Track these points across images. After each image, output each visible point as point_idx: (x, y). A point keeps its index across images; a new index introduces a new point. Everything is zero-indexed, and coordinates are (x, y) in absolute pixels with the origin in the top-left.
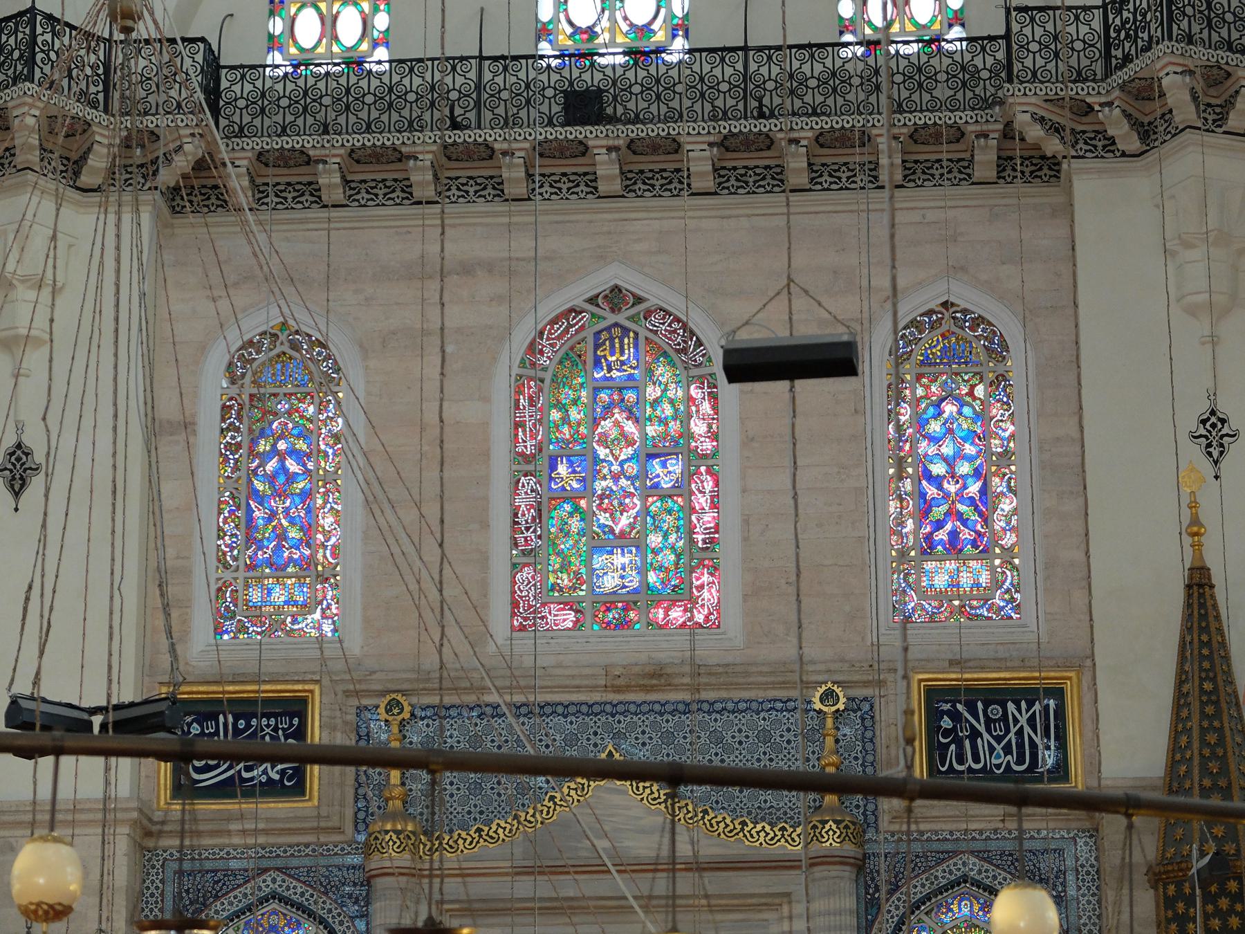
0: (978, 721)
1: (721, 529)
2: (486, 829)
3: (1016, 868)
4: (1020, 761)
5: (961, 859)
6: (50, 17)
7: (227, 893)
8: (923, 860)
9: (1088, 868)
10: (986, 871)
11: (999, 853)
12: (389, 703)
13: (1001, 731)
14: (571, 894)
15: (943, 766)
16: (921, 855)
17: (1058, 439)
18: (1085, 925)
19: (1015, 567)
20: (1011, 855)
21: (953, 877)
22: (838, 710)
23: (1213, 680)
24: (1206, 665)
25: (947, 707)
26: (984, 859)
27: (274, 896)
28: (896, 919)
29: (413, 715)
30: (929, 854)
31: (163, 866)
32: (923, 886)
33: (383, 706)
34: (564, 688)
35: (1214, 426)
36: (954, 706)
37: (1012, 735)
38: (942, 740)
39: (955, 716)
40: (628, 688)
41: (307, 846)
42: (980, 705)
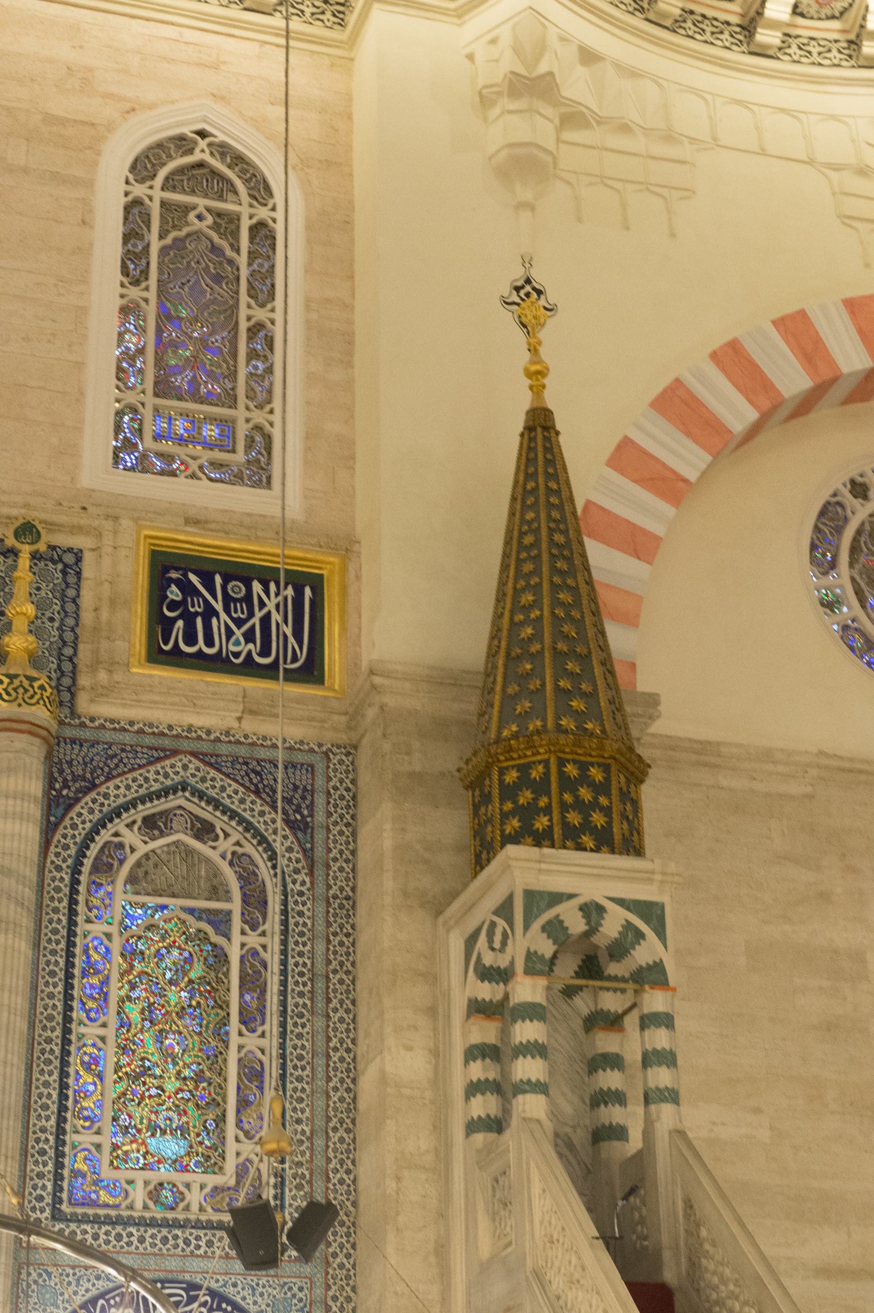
0: (215, 597)
3: (251, 780)
4: (265, 651)
5: (181, 760)
8: (130, 755)
10: (213, 779)
11: (230, 759)
13: (243, 613)
15: (166, 643)
16: (128, 748)
17: (328, 300)
18: (335, 860)
20: (246, 764)
21: (169, 782)
22: (37, 551)
23: (565, 532)
24: (555, 514)
25: (174, 575)
26: (211, 765)
28: (88, 825)
30: (139, 749)
32: (128, 787)
35: (528, 295)
36: (185, 576)
37: (256, 620)
38: (169, 614)
39: (187, 589)
42: (218, 579)
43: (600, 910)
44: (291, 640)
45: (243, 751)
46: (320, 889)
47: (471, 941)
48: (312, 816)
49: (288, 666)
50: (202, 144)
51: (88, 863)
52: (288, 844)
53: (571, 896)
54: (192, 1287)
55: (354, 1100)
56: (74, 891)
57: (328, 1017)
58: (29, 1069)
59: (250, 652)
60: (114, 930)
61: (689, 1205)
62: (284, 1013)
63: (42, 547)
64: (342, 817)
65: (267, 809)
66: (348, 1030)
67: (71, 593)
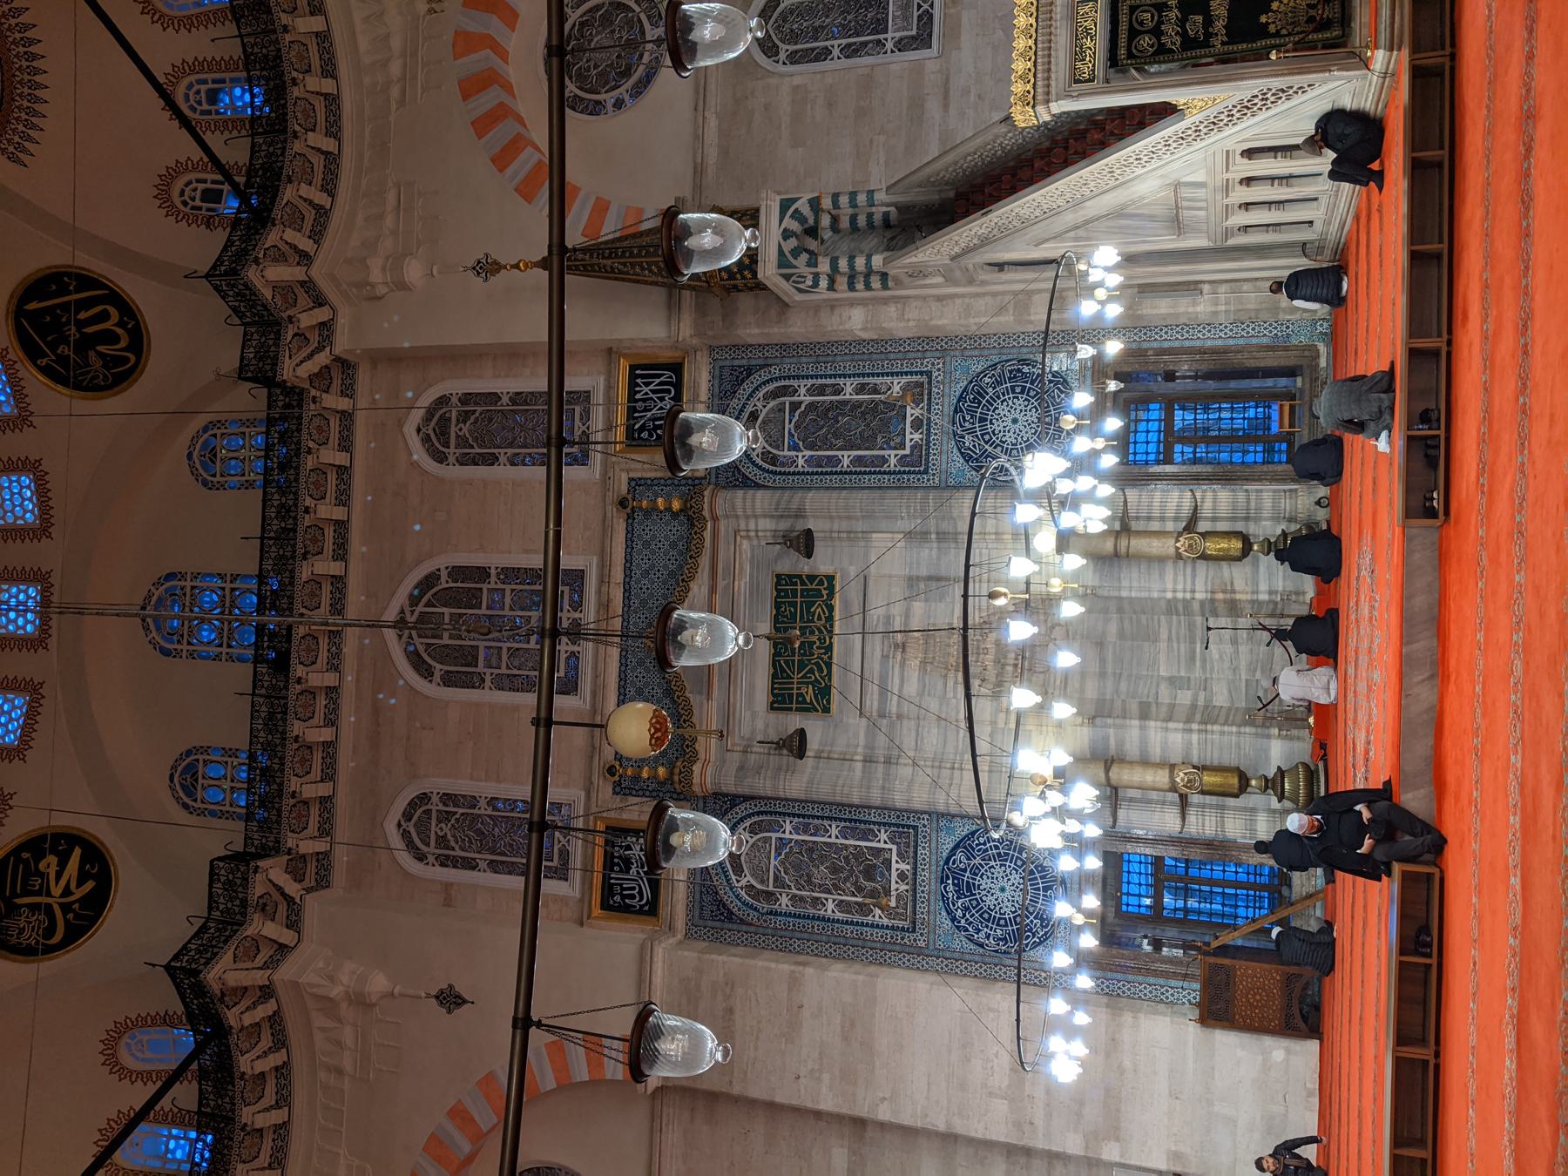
4: (669, 391)
6: (176, 957)
37: (654, 396)
39: (642, 428)
43: (785, 230)
46: (777, 361)
47: (800, 291)
50: (424, 430)
51: (771, 468)
53: (780, 245)
54: (956, 411)
56: (784, 473)
58: (863, 488)
60: (800, 455)
61: (920, 186)
62: (835, 376)
63: (630, 497)
67: (649, 482)
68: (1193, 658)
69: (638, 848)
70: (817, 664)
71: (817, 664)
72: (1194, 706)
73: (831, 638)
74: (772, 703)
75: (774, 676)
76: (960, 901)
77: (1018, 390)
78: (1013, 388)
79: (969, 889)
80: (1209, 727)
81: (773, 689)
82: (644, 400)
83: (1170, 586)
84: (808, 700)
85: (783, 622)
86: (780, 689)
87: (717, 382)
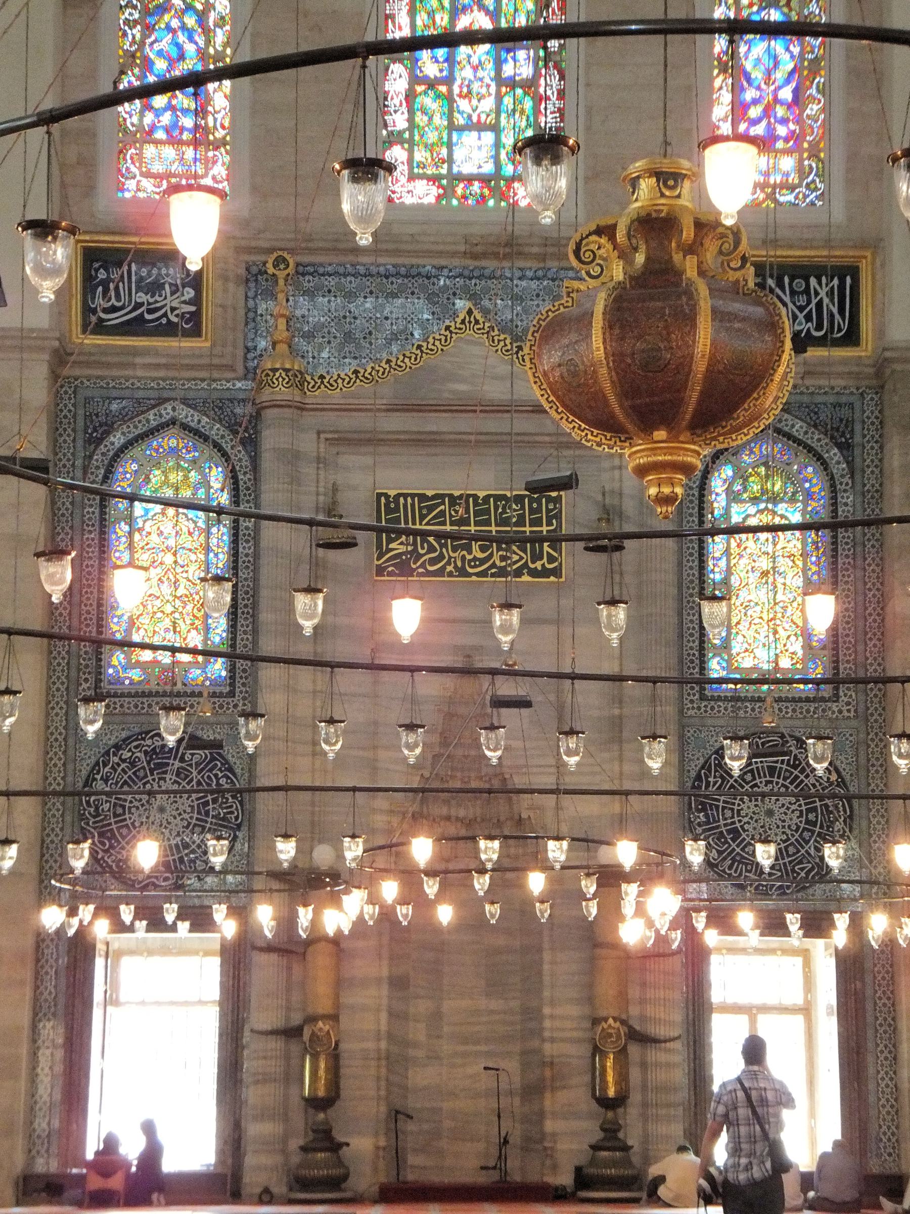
1: (566, 119)
2: (362, 371)
4: (819, 327)
7: (132, 418)
9: (873, 419)
12: (276, 259)
14: (434, 428)
18: (868, 466)
19: (819, 160)
20: (807, 407)
27: (173, 422)
29: (297, 273)
31: (75, 392)
33: (271, 261)
34: (430, 254)
37: (813, 305)
40: (484, 255)
41: (203, 380)
42: (786, 280)
44: (837, 316)
45: (806, 399)
46: (858, 487)
48: (852, 438)
49: (835, 336)
52: (836, 458)
55: (883, 620)
57: (865, 569)
58: (680, 614)
59: (809, 329)
64: (873, 437)
65: (822, 436)
66: (878, 577)
68: (465, 1041)
69: (175, 304)
70: (441, 557)
71: (441, 557)
72: (407, 1044)
73: (477, 575)
74: (387, 496)
75: (423, 497)
76: (141, 755)
77: (811, 817)
78: (814, 810)
79: (159, 766)
80: (384, 1063)
81: (405, 496)
82: (807, 291)
83: (559, 1011)
84: (391, 546)
85: (496, 508)
86: (405, 506)
87: (831, 399)
